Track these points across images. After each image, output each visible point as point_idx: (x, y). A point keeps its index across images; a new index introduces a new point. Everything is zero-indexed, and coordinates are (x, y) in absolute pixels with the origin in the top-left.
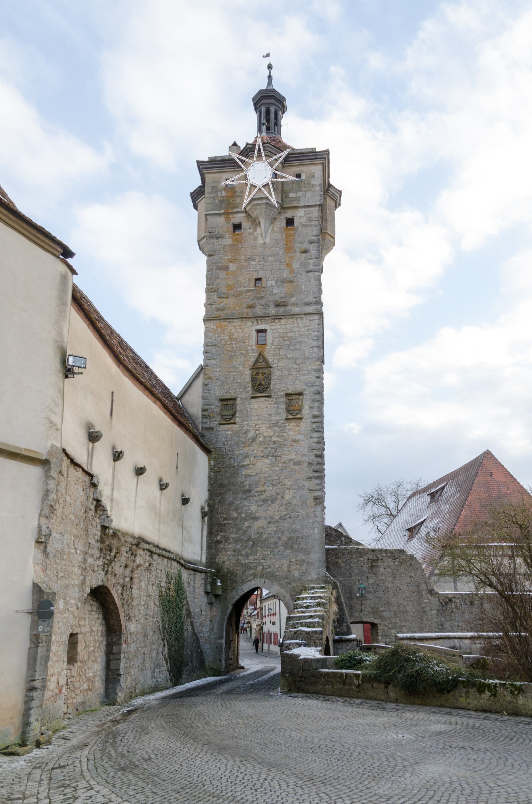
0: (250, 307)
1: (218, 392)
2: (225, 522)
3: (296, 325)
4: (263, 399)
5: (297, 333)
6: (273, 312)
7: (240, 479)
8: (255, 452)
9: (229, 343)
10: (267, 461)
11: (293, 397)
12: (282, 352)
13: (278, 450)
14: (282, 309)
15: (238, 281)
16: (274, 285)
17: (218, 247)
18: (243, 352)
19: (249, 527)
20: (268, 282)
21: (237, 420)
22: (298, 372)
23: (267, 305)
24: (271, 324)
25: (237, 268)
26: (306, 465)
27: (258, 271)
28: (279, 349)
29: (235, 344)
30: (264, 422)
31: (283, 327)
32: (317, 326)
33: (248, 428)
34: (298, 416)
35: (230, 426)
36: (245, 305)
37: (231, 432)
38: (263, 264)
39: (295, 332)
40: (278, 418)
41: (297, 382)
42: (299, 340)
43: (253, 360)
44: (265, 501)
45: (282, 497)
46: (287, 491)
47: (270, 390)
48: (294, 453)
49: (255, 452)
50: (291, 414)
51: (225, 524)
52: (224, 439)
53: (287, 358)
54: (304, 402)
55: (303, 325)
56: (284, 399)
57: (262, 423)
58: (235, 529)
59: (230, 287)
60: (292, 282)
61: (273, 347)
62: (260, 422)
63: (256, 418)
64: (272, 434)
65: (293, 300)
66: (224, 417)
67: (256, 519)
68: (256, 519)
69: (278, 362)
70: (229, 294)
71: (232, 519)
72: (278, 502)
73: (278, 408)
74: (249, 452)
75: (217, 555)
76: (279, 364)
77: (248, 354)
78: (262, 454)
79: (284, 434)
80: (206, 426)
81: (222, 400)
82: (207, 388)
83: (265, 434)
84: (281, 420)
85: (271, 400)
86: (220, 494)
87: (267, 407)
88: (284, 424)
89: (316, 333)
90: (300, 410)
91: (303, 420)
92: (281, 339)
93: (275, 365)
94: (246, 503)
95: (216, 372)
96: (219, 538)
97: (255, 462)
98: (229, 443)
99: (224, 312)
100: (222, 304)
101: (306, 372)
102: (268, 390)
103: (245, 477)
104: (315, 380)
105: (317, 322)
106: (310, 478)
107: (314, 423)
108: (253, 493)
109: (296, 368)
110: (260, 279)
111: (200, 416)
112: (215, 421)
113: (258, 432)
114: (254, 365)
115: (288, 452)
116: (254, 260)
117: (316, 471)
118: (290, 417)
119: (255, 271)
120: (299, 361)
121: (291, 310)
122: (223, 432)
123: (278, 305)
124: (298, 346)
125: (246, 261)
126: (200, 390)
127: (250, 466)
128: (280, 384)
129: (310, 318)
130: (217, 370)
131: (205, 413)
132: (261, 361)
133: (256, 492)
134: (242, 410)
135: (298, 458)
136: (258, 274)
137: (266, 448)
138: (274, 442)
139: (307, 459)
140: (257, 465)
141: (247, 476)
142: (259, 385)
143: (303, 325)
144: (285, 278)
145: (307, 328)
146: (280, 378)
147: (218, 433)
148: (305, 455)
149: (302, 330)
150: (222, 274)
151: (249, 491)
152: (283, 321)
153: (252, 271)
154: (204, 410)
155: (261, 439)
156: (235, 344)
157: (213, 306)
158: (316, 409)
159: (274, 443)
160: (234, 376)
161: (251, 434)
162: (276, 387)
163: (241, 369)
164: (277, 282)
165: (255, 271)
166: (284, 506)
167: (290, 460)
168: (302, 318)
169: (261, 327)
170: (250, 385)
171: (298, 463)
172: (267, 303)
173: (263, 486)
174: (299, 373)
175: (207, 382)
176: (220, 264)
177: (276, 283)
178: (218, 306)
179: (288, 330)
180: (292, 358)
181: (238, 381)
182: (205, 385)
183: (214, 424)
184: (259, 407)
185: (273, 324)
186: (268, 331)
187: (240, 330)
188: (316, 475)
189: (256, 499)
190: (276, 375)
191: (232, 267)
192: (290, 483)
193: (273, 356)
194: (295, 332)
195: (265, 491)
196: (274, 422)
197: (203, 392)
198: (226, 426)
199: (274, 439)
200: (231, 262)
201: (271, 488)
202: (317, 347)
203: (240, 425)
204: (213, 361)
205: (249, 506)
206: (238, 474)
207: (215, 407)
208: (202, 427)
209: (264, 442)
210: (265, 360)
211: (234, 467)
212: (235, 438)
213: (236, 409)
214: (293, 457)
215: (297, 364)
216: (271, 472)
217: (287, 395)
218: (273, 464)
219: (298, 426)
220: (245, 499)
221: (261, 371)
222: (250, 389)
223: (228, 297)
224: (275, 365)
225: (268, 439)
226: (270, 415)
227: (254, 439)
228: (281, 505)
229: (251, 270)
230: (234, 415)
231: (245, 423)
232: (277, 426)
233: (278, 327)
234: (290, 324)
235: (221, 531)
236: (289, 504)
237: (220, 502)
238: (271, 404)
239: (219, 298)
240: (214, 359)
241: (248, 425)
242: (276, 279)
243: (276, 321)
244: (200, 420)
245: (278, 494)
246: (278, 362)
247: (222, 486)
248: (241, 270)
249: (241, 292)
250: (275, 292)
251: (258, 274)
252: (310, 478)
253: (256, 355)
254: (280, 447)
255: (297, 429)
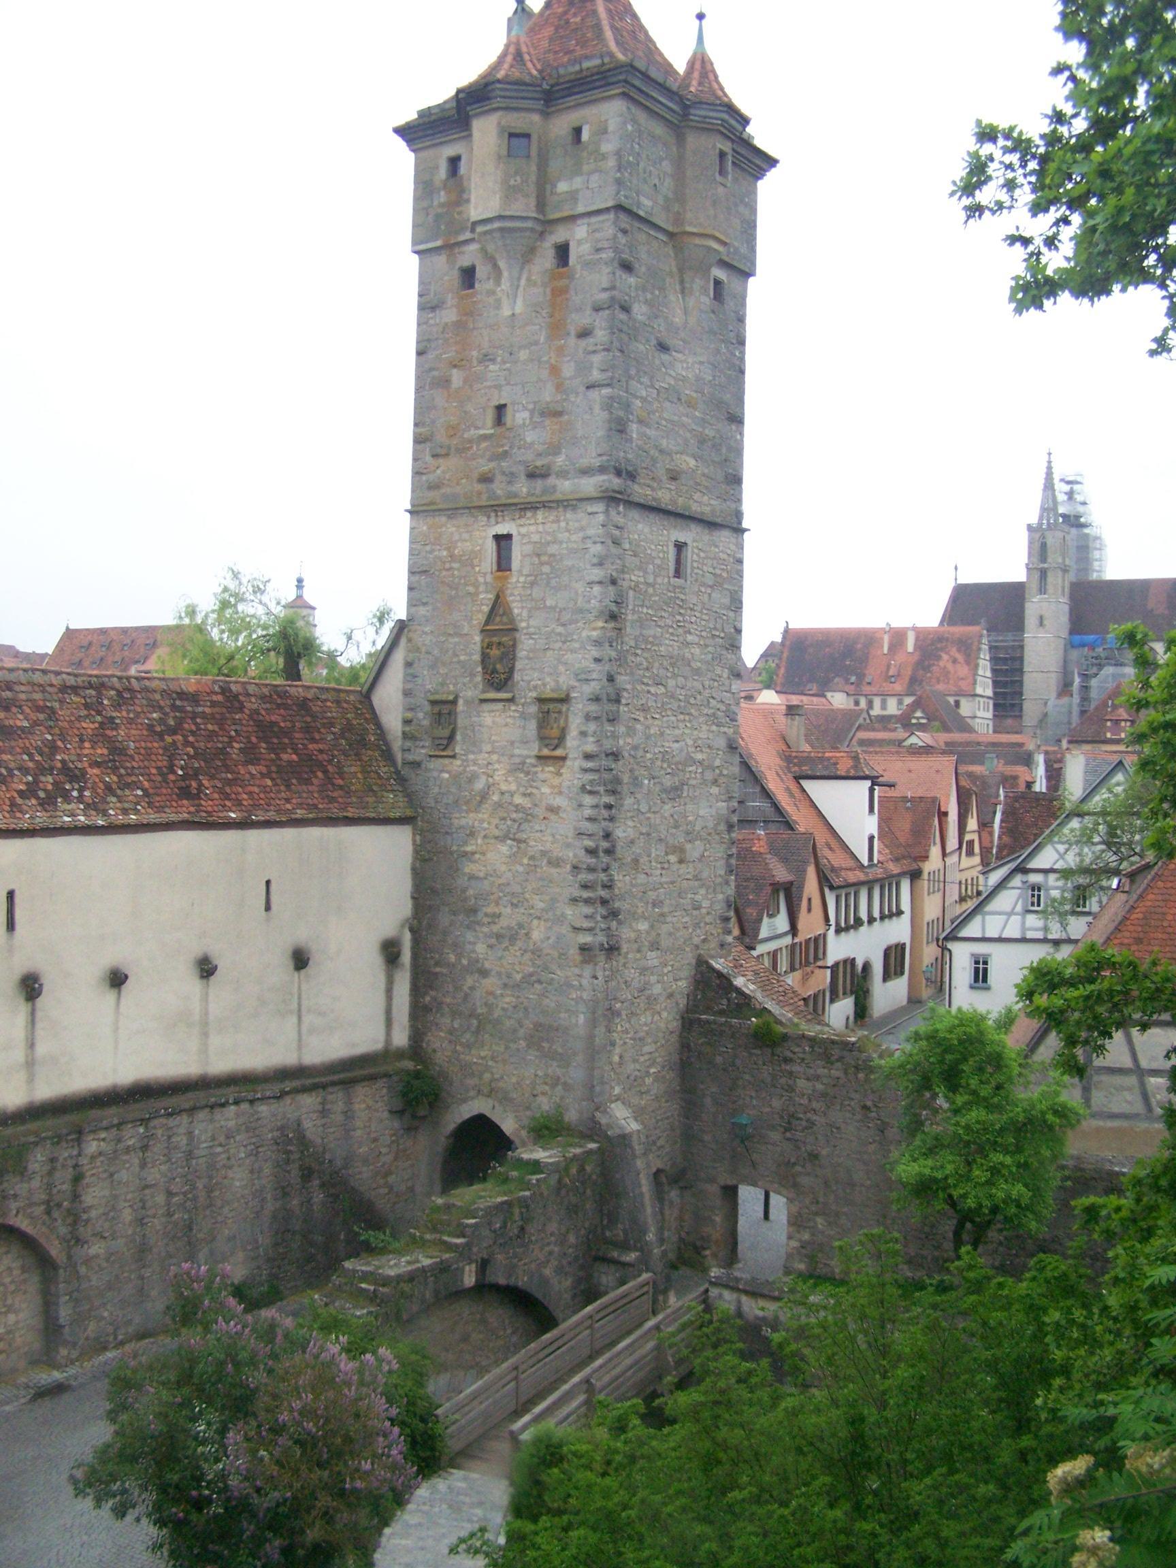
0: (486, 479)
1: (429, 682)
2: (438, 970)
3: (563, 524)
4: (500, 706)
5: (564, 545)
6: (524, 490)
7: (462, 881)
8: (485, 825)
9: (447, 566)
10: (504, 849)
11: (551, 706)
12: (537, 592)
13: (522, 827)
14: (539, 484)
15: (465, 412)
16: (528, 422)
17: (435, 330)
18: (471, 589)
19: (472, 988)
20: (517, 415)
21: (458, 750)
22: (564, 642)
23: (512, 474)
24: (519, 522)
25: (465, 381)
26: (569, 867)
27: (498, 387)
28: (532, 584)
29: (458, 570)
30: (502, 759)
31: (541, 528)
32: (601, 531)
33: (476, 768)
34: (558, 752)
35: (446, 761)
36: (476, 475)
37: (446, 776)
38: (508, 370)
39: (561, 543)
40: (525, 752)
41: (562, 668)
42: (569, 563)
43: (486, 609)
44: (499, 937)
45: (527, 934)
46: (535, 922)
47: (513, 686)
48: (550, 839)
49: (485, 825)
50: (547, 746)
51: (436, 974)
52: (436, 790)
53: (545, 607)
54: (571, 719)
55: (576, 525)
56: (533, 709)
57: (499, 762)
58: (451, 989)
59: (453, 431)
60: (558, 414)
61: (522, 579)
62: (495, 757)
63: (488, 748)
64: (513, 787)
65: (560, 460)
66: (437, 742)
67: (484, 973)
68: (484, 973)
69: (530, 617)
70: (449, 448)
71: (448, 965)
72: (519, 944)
73: (524, 727)
74: (476, 824)
75: (424, 1034)
76: (532, 622)
77: (477, 594)
78: (497, 833)
79: (534, 791)
80: (411, 757)
81: (434, 703)
82: (411, 671)
83: (504, 787)
84: (529, 757)
85: (513, 708)
86: (430, 907)
87: (506, 725)
88: (535, 766)
89: (599, 547)
90: (561, 739)
91: (568, 763)
92: (536, 560)
93: (524, 624)
94: (470, 936)
95: (426, 633)
96: (428, 999)
97: (485, 847)
98: (445, 801)
99: (443, 491)
100: (438, 472)
101: (577, 645)
102: (510, 683)
103: (469, 879)
104: (593, 666)
105: (601, 518)
106: (574, 900)
107: (586, 770)
108: (480, 915)
109: (560, 634)
110: (501, 409)
111: (400, 734)
112: (423, 747)
113: (490, 780)
114: (487, 623)
115: (539, 834)
116: (493, 361)
117: (585, 887)
118: (546, 752)
119: (495, 387)
120: (566, 617)
121: (554, 487)
122: (435, 774)
123: (531, 475)
124: (566, 579)
125: (480, 362)
126: (400, 676)
127: (477, 856)
128: (535, 673)
129: (590, 509)
130: (427, 629)
131: (407, 729)
132: (501, 611)
133: (486, 915)
134: (466, 728)
135: (557, 852)
136: (500, 397)
137: (504, 819)
138: (517, 806)
139: (571, 855)
140: (489, 855)
141: (472, 877)
142: (492, 673)
143: (576, 525)
144: (548, 403)
145: (581, 535)
146: (531, 655)
147: (428, 775)
148: (568, 845)
149: (574, 538)
150: (440, 398)
151: (474, 911)
152: (540, 515)
153: (490, 387)
154: (407, 722)
155: (495, 798)
156: (458, 570)
157: (424, 478)
158: (591, 739)
159: (518, 809)
160: (456, 644)
161: (480, 785)
162: (525, 678)
163: (465, 631)
164: (532, 412)
165: (495, 387)
166: (528, 956)
167: (544, 853)
168: (574, 508)
169: (502, 529)
170: (480, 669)
171: (555, 863)
172: (514, 470)
173: (497, 904)
174: (565, 647)
175: (411, 657)
176: (436, 373)
177: (531, 419)
178: (431, 477)
179: (549, 538)
180: (553, 608)
181: (462, 658)
182: (409, 664)
183: (419, 754)
184: (494, 722)
185: (522, 521)
186: (514, 539)
187: (466, 536)
188: (586, 894)
189: (485, 929)
190: (525, 646)
191: (457, 377)
192: (541, 905)
193: (521, 601)
194: (561, 543)
195: (499, 916)
196: (517, 760)
197: (405, 681)
198: (441, 760)
199: (518, 800)
200: (455, 366)
201: (509, 910)
202: (600, 583)
203: (463, 761)
204: (421, 608)
205: (475, 943)
206: (458, 870)
207: (423, 717)
208: (403, 759)
209: (499, 805)
210: (508, 612)
211: (452, 853)
212: (453, 790)
213: (455, 723)
214: (548, 846)
215: (563, 625)
216: (509, 875)
217: (541, 701)
218: (513, 858)
219: (559, 774)
220: (468, 927)
221: (495, 639)
222: (479, 678)
223: (447, 455)
224: (524, 624)
225: (507, 797)
226: (512, 743)
227: (484, 796)
228: (525, 951)
229: (488, 384)
230: (451, 738)
231: (471, 757)
232: (522, 771)
233: (532, 528)
234: (553, 522)
235: (431, 988)
236: (537, 952)
237: (430, 926)
238: (514, 717)
239: (433, 456)
240: (425, 604)
241: (475, 764)
242: (531, 406)
243: (529, 514)
244: (400, 743)
245: (520, 926)
246: (530, 617)
247: (434, 891)
248: (471, 386)
249: (470, 441)
250: (529, 440)
251: (500, 397)
252: (574, 900)
253: (492, 596)
254: (526, 820)
255: (556, 781)
